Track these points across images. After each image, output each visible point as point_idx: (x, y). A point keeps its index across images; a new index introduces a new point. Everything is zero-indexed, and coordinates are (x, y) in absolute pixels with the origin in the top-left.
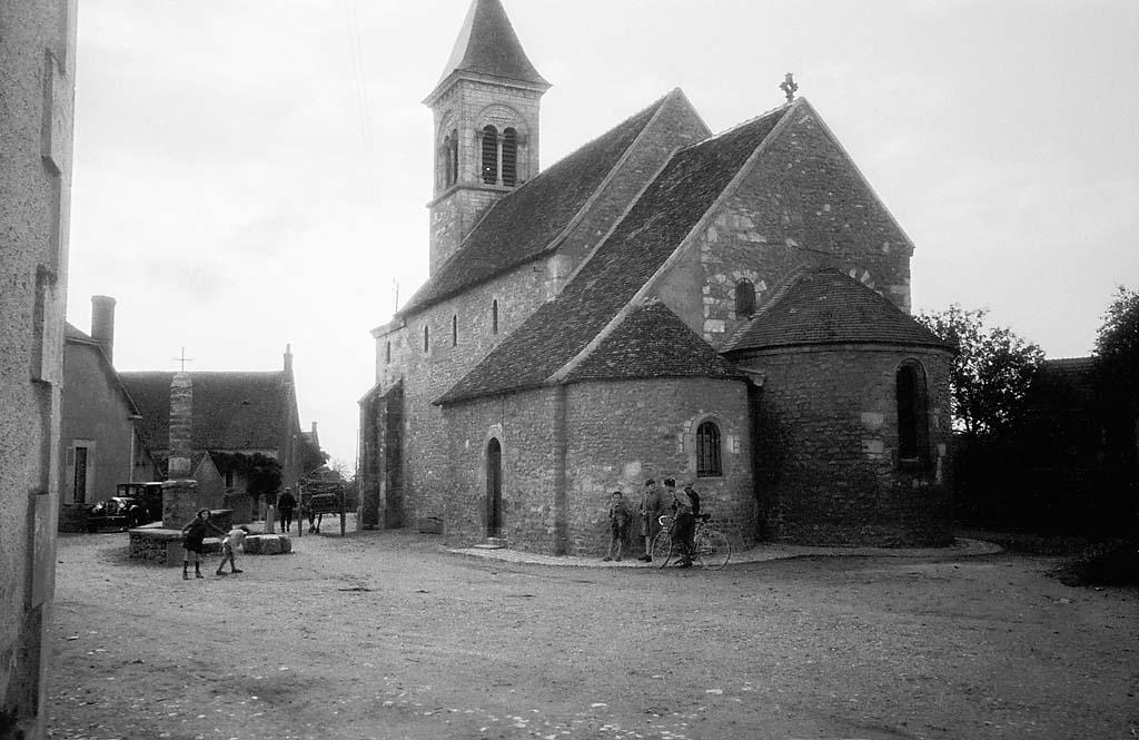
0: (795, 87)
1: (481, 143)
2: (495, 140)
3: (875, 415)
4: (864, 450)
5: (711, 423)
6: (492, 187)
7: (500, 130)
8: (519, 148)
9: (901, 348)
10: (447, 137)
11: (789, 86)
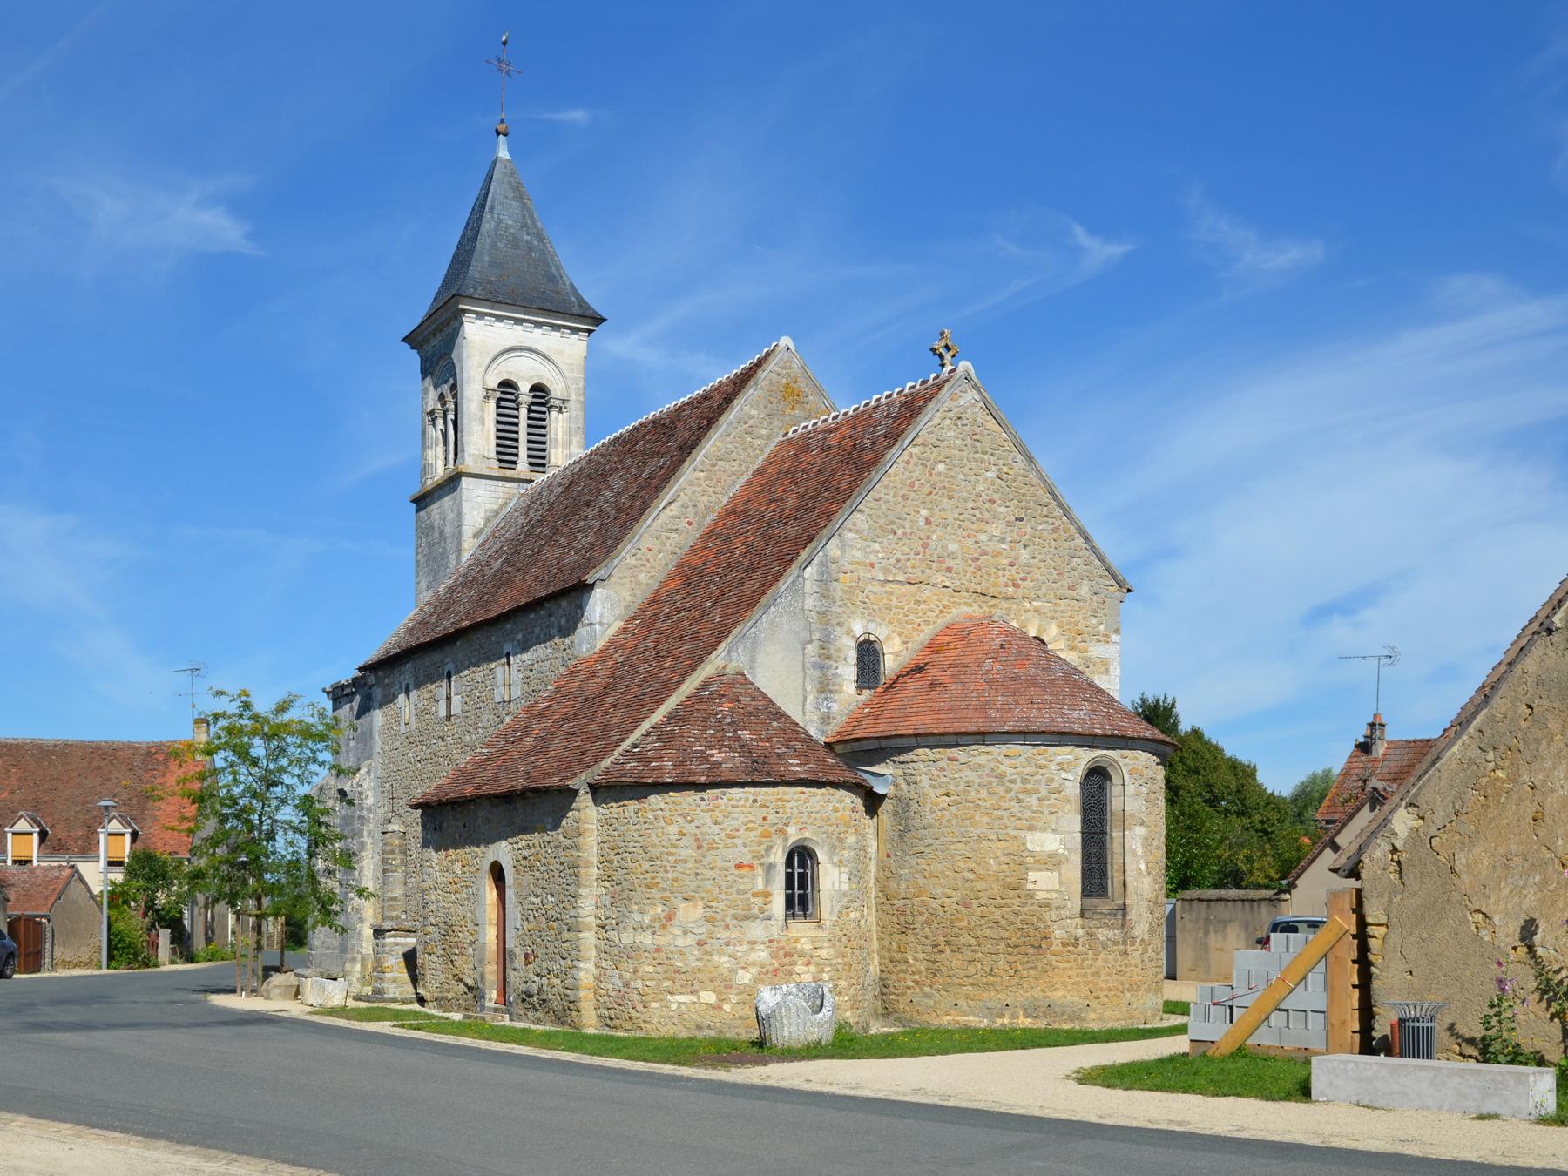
1: (492, 405)
3: (1052, 835)
4: (1030, 886)
5: (805, 848)
6: (509, 473)
7: (524, 387)
8: (554, 413)
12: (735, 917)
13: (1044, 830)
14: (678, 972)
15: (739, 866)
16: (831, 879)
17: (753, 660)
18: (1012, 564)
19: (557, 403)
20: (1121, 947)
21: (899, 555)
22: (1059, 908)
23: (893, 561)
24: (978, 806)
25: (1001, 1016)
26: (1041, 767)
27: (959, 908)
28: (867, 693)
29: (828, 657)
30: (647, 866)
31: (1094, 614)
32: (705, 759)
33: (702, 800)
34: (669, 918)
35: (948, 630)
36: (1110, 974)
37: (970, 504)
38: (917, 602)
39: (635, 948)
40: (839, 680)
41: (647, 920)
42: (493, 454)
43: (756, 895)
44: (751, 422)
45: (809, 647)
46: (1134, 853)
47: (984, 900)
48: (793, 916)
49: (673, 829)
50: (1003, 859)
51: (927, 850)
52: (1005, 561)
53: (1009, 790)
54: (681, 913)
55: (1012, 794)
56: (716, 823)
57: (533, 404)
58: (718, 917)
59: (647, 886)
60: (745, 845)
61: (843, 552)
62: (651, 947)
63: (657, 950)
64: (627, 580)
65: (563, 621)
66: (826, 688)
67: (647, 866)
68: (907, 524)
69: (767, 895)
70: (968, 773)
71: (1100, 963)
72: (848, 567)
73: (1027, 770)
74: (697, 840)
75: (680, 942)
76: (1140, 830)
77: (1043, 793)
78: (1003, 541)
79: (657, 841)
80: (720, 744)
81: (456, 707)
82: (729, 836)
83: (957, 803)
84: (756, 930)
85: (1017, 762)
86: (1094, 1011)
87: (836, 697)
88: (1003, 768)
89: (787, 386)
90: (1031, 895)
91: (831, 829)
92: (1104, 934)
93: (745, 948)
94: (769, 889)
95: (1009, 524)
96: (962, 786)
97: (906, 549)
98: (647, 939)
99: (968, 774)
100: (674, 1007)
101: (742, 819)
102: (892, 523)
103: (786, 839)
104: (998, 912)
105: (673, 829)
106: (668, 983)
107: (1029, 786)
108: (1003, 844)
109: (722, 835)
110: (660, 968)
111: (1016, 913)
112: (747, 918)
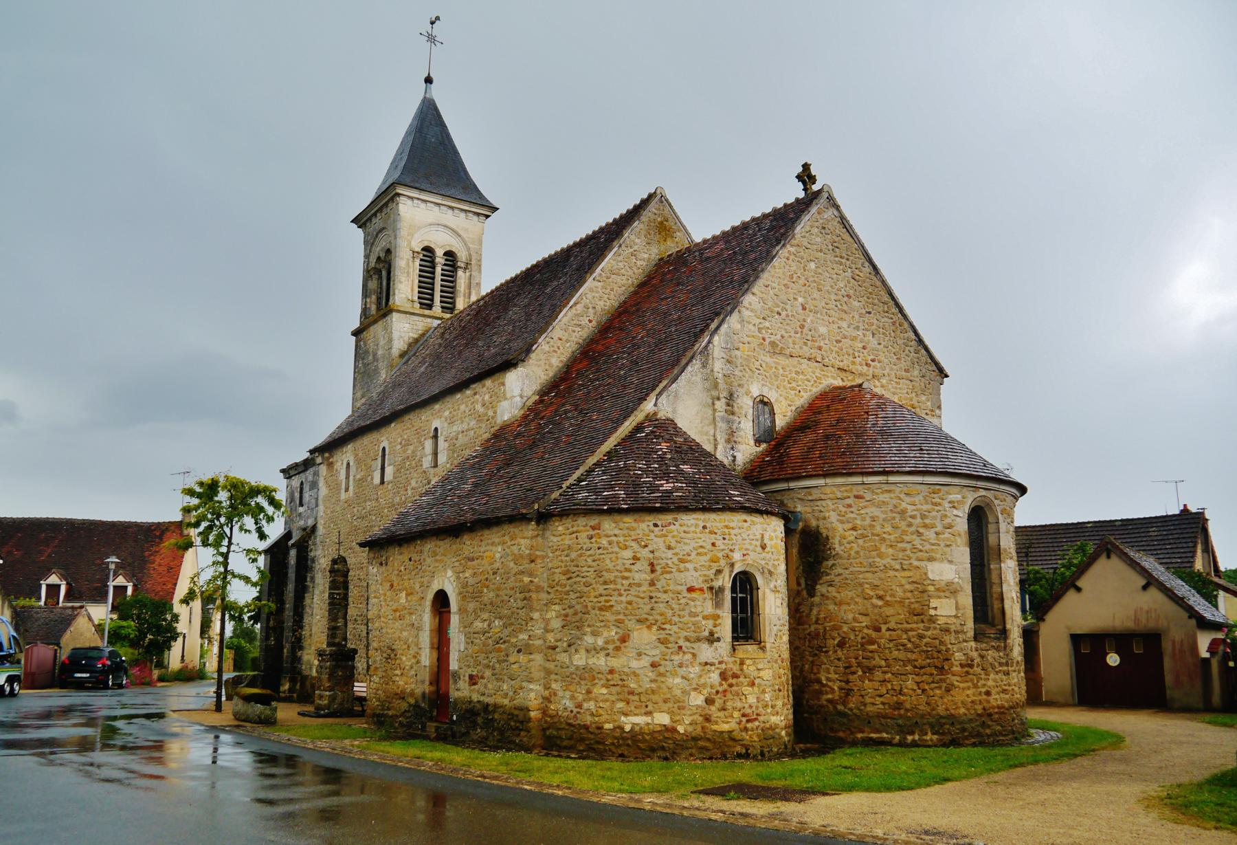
0: (813, 179)
1: (418, 262)
3: (946, 566)
4: (932, 612)
6: (427, 312)
7: (440, 253)
8: (460, 273)
9: (973, 483)
10: (379, 258)
11: (806, 176)
12: (687, 639)
13: (942, 561)
15: (691, 590)
17: (674, 411)
18: (864, 348)
22: (957, 632)
23: (779, 337)
24: (883, 539)
25: (912, 733)
26: (936, 504)
27: (870, 632)
28: (764, 446)
29: (733, 414)
30: (601, 589)
32: (655, 489)
33: (656, 525)
34: (624, 640)
35: (823, 395)
37: (833, 297)
38: (797, 373)
40: (742, 433)
41: (600, 642)
42: (416, 298)
43: (705, 618)
44: (636, 248)
45: (717, 402)
47: (892, 625)
49: (628, 554)
50: (908, 587)
51: (837, 579)
52: (861, 345)
53: (910, 525)
54: (635, 635)
55: (913, 529)
56: (669, 548)
58: (672, 639)
59: (601, 609)
60: (696, 570)
62: (605, 669)
63: (611, 672)
65: (487, 397)
66: (731, 439)
67: (601, 589)
68: (788, 307)
69: (716, 617)
70: (873, 509)
71: (990, 683)
72: (746, 339)
73: (925, 507)
74: (652, 564)
75: (634, 664)
78: (857, 328)
79: (610, 565)
80: (666, 476)
81: (389, 475)
82: (681, 561)
83: (863, 536)
84: (706, 652)
86: (989, 727)
88: (904, 505)
89: (661, 223)
90: (932, 620)
92: (991, 654)
93: (697, 669)
95: (861, 315)
96: (868, 521)
98: (600, 662)
100: (628, 728)
101: (693, 544)
103: (732, 565)
104: (905, 636)
105: (628, 554)
106: (620, 705)
108: (907, 574)
109: (675, 559)
110: (614, 690)
111: (921, 637)
112: (699, 640)
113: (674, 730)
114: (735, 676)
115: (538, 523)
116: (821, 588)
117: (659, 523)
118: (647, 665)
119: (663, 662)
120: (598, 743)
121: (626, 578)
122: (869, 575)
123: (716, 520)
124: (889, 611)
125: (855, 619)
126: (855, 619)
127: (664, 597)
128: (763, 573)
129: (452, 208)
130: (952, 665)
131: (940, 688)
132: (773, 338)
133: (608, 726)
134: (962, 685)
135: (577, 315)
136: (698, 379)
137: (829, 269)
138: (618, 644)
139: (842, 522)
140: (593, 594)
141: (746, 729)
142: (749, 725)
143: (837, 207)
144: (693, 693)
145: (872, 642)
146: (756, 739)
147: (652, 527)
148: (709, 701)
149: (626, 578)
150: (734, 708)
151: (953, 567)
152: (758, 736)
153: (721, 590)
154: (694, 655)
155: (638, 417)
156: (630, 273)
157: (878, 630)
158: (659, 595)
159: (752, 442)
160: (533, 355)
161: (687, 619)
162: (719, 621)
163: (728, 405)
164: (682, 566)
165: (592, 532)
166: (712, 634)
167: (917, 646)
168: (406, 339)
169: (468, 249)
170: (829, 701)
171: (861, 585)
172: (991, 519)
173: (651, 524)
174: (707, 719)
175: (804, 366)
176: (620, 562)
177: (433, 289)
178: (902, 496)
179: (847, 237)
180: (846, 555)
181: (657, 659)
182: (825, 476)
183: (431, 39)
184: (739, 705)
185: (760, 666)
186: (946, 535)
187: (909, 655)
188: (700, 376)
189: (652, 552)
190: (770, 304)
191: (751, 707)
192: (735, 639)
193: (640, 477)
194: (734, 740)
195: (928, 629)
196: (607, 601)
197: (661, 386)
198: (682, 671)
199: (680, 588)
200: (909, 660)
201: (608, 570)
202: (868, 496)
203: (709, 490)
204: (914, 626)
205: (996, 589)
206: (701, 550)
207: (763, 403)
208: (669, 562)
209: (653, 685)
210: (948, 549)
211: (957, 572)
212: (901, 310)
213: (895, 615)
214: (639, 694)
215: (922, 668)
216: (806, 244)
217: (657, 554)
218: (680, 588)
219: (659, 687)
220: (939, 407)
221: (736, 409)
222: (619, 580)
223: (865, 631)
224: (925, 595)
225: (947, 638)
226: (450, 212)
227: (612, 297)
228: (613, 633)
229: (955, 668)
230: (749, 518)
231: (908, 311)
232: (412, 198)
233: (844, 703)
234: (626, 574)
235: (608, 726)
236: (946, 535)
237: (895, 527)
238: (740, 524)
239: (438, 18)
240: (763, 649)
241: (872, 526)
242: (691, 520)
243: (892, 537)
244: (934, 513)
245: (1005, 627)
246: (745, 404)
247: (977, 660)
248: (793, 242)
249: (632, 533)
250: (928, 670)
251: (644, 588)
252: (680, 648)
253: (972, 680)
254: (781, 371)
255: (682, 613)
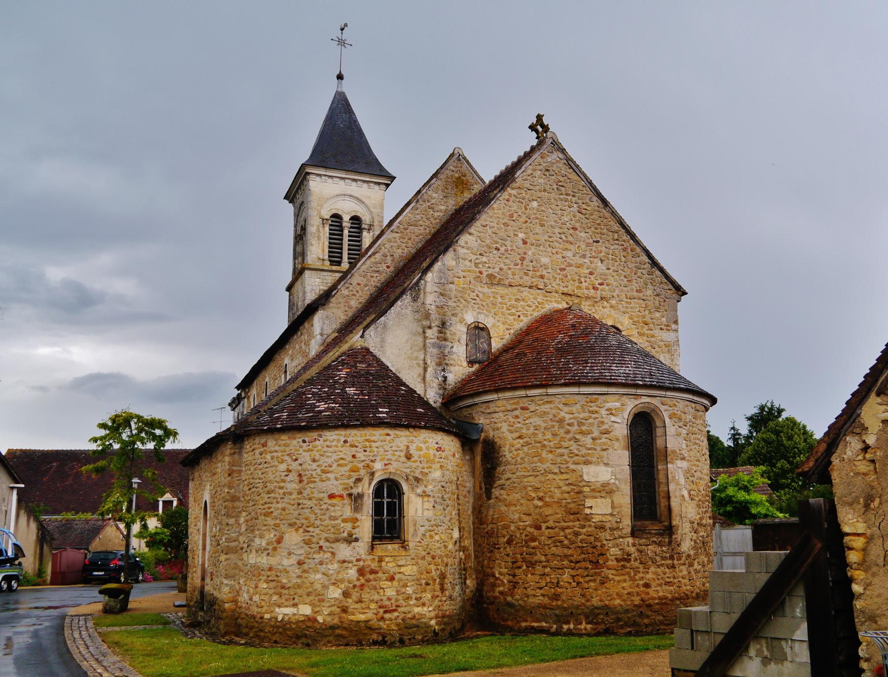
0: (546, 128)
1: (327, 228)
2: (341, 226)
3: (602, 468)
4: (588, 511)
6: (334, 268)
7: (346, 218)
8: (365, 233)
11: (539, 126)
12: (327, 540)
14: (283, 587)
15: (331, 496)
16: (416, 508)
17: (383, 341)
18: (591, 273)
19: (366, 227)
20: (670, 562)
21: (502, 266)
22: (612, 529)
23: (497, 270)
24: (544, 446)
25: (568, 623)
26: (592, 412)
27: (532, 530)
28: (476, 366)
29: (445, 340)
31: (657, 309)
33: (304, 441)
34: (279, 541)
36: (660, 585)
37: (557, 230)
38: (517, 300)
39: (255, 567)
40: (455, 356)
42: (326, 257)
44: (433, 201)
45: (429, 333)
46: (678, 484)
48: (381, 539)
49: (283, 467)
51: (508, 483)
52: (587, 271)
53: (568, 432)
54: (287, 537)
55: (571, 435)
56: (314, 461)
57: (351, 227)
58: (314, 540)
59: (265, 515)
60: (336, 479)
61: (458, 263)
62: (266, 566)
63: (270, 569)
64: (342, 305)
66: (443, 363)
68: (508, 243)
71: (650, 576)
72: (462, 274)
73: (582, 415)
74: (300, 475)
75: (286, 562)
76: (684, 464)
77: (596, 434)
78: (584, 256)
82: (324, 472)
83: (528, 444)
84: (344, 551)
85: (574, 409)
86: (648, 617)
87: (452, 368)
88: (562, 414)
90: (588, 518)
91: (414, 465)
93: (336, 566)
94: (358, 516)
95: (588, 245)
96: (532, 430)
97: (507, 261)
99: (536, 420)
100: (280, 618)
101: (335, 457)
102: (497, 243)
103: (372, 474)
104: (562, 534)
105: (283, 467)
106: (275, 598)
107: (584, 428)
108: (565, 476)
110: (272, 584)
111: (577, 534)
112: (337, 540)
113: (316, 620)
114: (373, 572)
115: (234, 443)
116: (496, 492)
117: (307, 439)
118: (295, 562)
119: (307, 561)
120: (261, 631)
121: (281, 488)
122: (531, 479)
123: (357, 435)
124: (548, 511)
125: (520, 519)
126: (520, 519)
127: (308, 503)
128: (407, 480)
129: (354, 180)
130: (607, 560)
131: (595, 581)
132: (490, 271)
133: (267, 616)
134: (617, 578)
135: (376, 263)
136: (409, 311)
137: (554, 206)
138: (275, 545)
139: (511, 432)
140: (262, 502)
141: (382, 618)
142: (387, 616)
143: (563, 151)
144: (331, 588)
145: (534, 539)
146: (395, 628)
147: (301, 443)
148: (346, 594)
149: (281, 488)
150: (372, 601)
151: (610, 469)
152: (398, 625)
153: (360, 496)
154: (333, 554)
155: (345, 347)
156: (428, 223)
157: (538, 528)
158: (305, 502)
159: (465, 364)
160: (333, 300)
161: (327, 522)
162: (358, 523)
163: (440, 332)
164: (324, 476)
165: (262, 449)
166: (350, 535)
167: (572, 543)
168: (317, 291)
169: (371, 213)
170: (501, 593)
171: (525, 487)
172: (658, 423)
173: (300, 440)
174: (345, 610)
175: (525, 294)
176: (278, 474)
177: (341, 249)
178: (561, 406)
179: (573, 176)
180: (513, 461)
181: (302, 558)
182: (497, 390)
183: (342, 42)
184: (376, 597)
185: (400, 563)
186: (603, 440)
187: (566, 551)
188: (410, 308)
189: (301, 465)
190: (488, 242)
191: (389, 599)
192: (374, 538)
193: (309, 399)
194: (370, 628)
195: (583, 527)
196: (269, 508)
197: (369, 320)
198: (323, 568)
199: (322, 495)
200: (566, 556)
201: (271, 482)
202: (532, 408)
203: (405, 410)
204: (570, 524)
205: (663, 488)
206: (341, 462)
207: (478, 331)
208: (314, 473)
209: (299, 581)
210: (605, 453)
211: (613, 474)
212: (633, 236)
213: (554, 514)
214: (289, 588)
215: (577, 562)
216: (528, 186)
217: (304, 466)
218: (322, 495)
219: (303, 582)
220: (676, 322)
221: (448, 335)
222: (277, 490)
223: (528, 529)
224: (580, 495)
225: (604, 535)
226: (354, 184)
227: (410, 245)
228: (271, 536)
229: (610, 563)
230: (392, 432)
231: (640, 236)
232: (320, 175)
233: (512, 595)
234: (282, 484)
235: (267, 616)
236: (603, 440)
237: (555, 435)
238: (382, 438)
239: (346, 25)
240: (404, 546)
241: (534, 434)
242: (333, 437)
243: (552, 444)
244: (591, 421)
245: (670, 523)
246: (459, 331)
247: (636, 554)
248: (514, 185)
249: (287, 449)
250: (583, 564)
251: (294, 496)
252: (321, 547)
253: (628, 574)
254: (500, 300)
255: (323, 517)
